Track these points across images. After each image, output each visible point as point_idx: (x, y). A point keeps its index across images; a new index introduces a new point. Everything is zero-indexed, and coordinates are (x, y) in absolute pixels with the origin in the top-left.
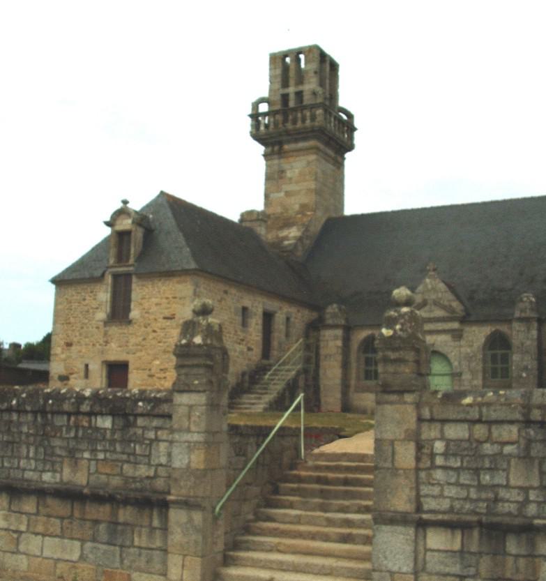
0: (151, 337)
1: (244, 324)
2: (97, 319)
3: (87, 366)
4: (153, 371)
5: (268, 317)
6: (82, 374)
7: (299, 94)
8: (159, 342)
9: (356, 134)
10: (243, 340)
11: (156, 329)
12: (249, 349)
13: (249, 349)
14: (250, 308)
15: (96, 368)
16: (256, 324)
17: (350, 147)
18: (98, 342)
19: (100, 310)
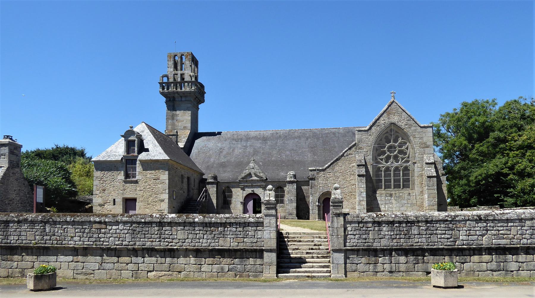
0: (147, 187)
1: (182, 182)
2: (119, 179)
3: (114, 200)
4: (149, 202)
5: (188, 178)
6: (112, 203)
7: (182, 75)
8: (152, 190)
9: (205, 95)
10: (182, 188)
11: (150, 184)
12: (184, 192)
13: (184, 192)
14: (184, 175)
15: (119, 201)
16: (185, 180)
17: (203, 101)
18: (120, 189)
19: (120, 175)
